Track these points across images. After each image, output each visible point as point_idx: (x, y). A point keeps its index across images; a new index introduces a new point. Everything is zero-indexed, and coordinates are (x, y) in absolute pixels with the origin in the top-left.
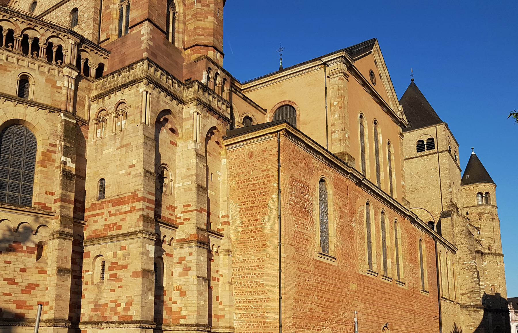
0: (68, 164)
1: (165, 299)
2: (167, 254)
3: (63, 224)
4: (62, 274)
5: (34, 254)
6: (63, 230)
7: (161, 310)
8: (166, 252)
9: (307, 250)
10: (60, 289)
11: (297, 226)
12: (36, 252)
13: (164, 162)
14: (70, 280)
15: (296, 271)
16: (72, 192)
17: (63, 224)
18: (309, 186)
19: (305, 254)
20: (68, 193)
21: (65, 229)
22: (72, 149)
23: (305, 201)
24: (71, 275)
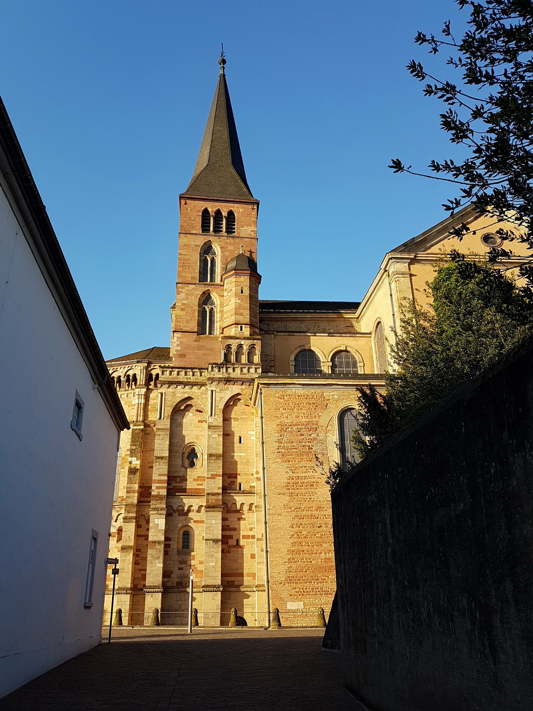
0: (133, 463)
1: (193, 563)
2: (195, 522)
3: (127, 511)
4: (125, 551)
5: (115, 537)
6: (127, 515)
7: (188, 574)
8: (195, 520)
9: (316, 493)
10: (123, 563)
11: (292, 473)
12: (117, 536)
13: (190, 441)
14: (131, 555)
15: (291, 520)
16: (135, 483)
17: (127, 511)
18: (317, 424)
19: (310, 499)
20: (133, 485)
21: (129, 514)
22: (137, 450)
23: (308, 442)
24: (132, 551)
